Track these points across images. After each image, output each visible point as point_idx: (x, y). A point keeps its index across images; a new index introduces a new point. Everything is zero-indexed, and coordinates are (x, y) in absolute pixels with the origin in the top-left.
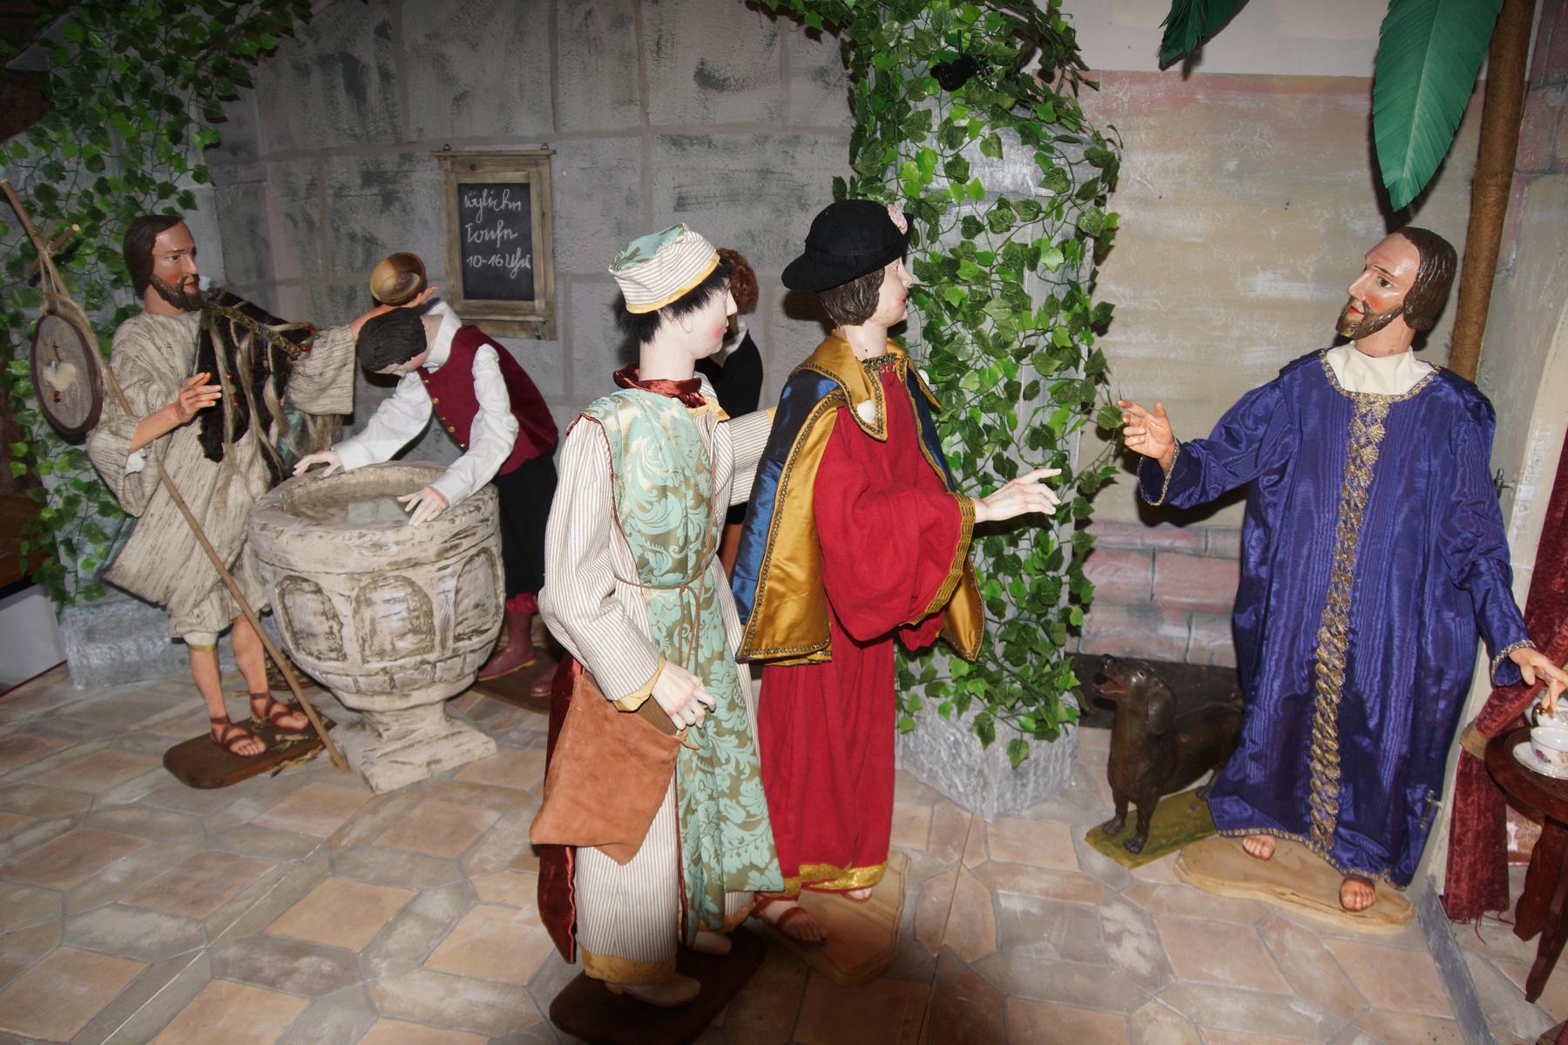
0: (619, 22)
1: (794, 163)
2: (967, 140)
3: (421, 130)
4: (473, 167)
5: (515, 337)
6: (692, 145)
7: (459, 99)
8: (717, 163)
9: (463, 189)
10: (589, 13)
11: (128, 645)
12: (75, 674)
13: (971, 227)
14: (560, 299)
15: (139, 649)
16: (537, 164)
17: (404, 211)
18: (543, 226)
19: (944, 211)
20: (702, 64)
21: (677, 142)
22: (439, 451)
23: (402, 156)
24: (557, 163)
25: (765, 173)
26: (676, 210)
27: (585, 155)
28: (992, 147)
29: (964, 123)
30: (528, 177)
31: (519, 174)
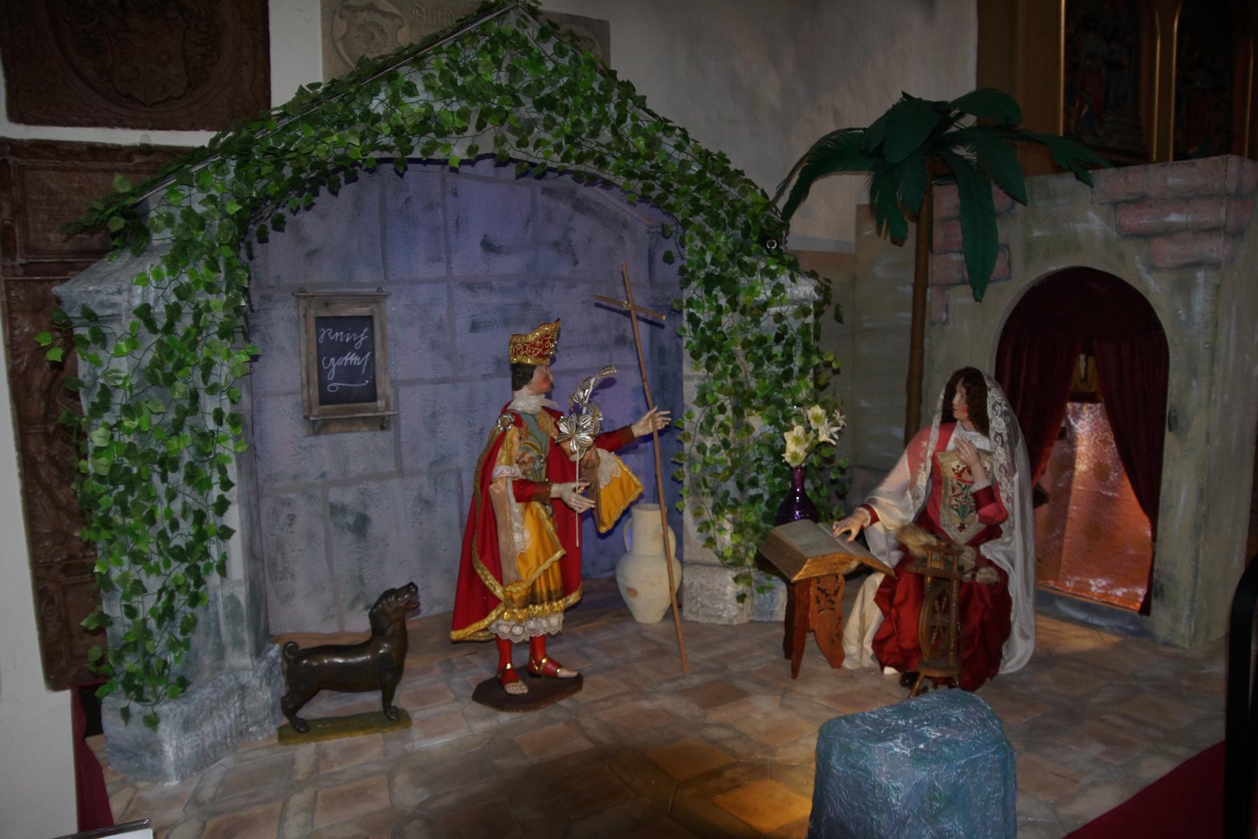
0: (430, 207)
1: (542, 299)
2: (778, 276)
3: (278, 277)
4: (327, 305)
5: (358, 431)
6: (480, 288)
7: (311, 255)
8: (496, 300)
9: (321, 322)
10: (408, 199)
11: (207, 728)
12: (171, 770)
13: (779, 317)
14: (392, 399)
15: (214, 731)
16: (377, 302)
17: (264, 340)
18: (383, 347)
19: (765, 310)
20: (486, 236)
21: (470, 286)
22: (292, 532)
23: (262, 297)
24: (389, 302)
25: (526, 305)
26: (471, 331)
27: (407, 296)
28: (793, 279)
29: (773, 267)
30: (372, 311)
31: (365, 309)
